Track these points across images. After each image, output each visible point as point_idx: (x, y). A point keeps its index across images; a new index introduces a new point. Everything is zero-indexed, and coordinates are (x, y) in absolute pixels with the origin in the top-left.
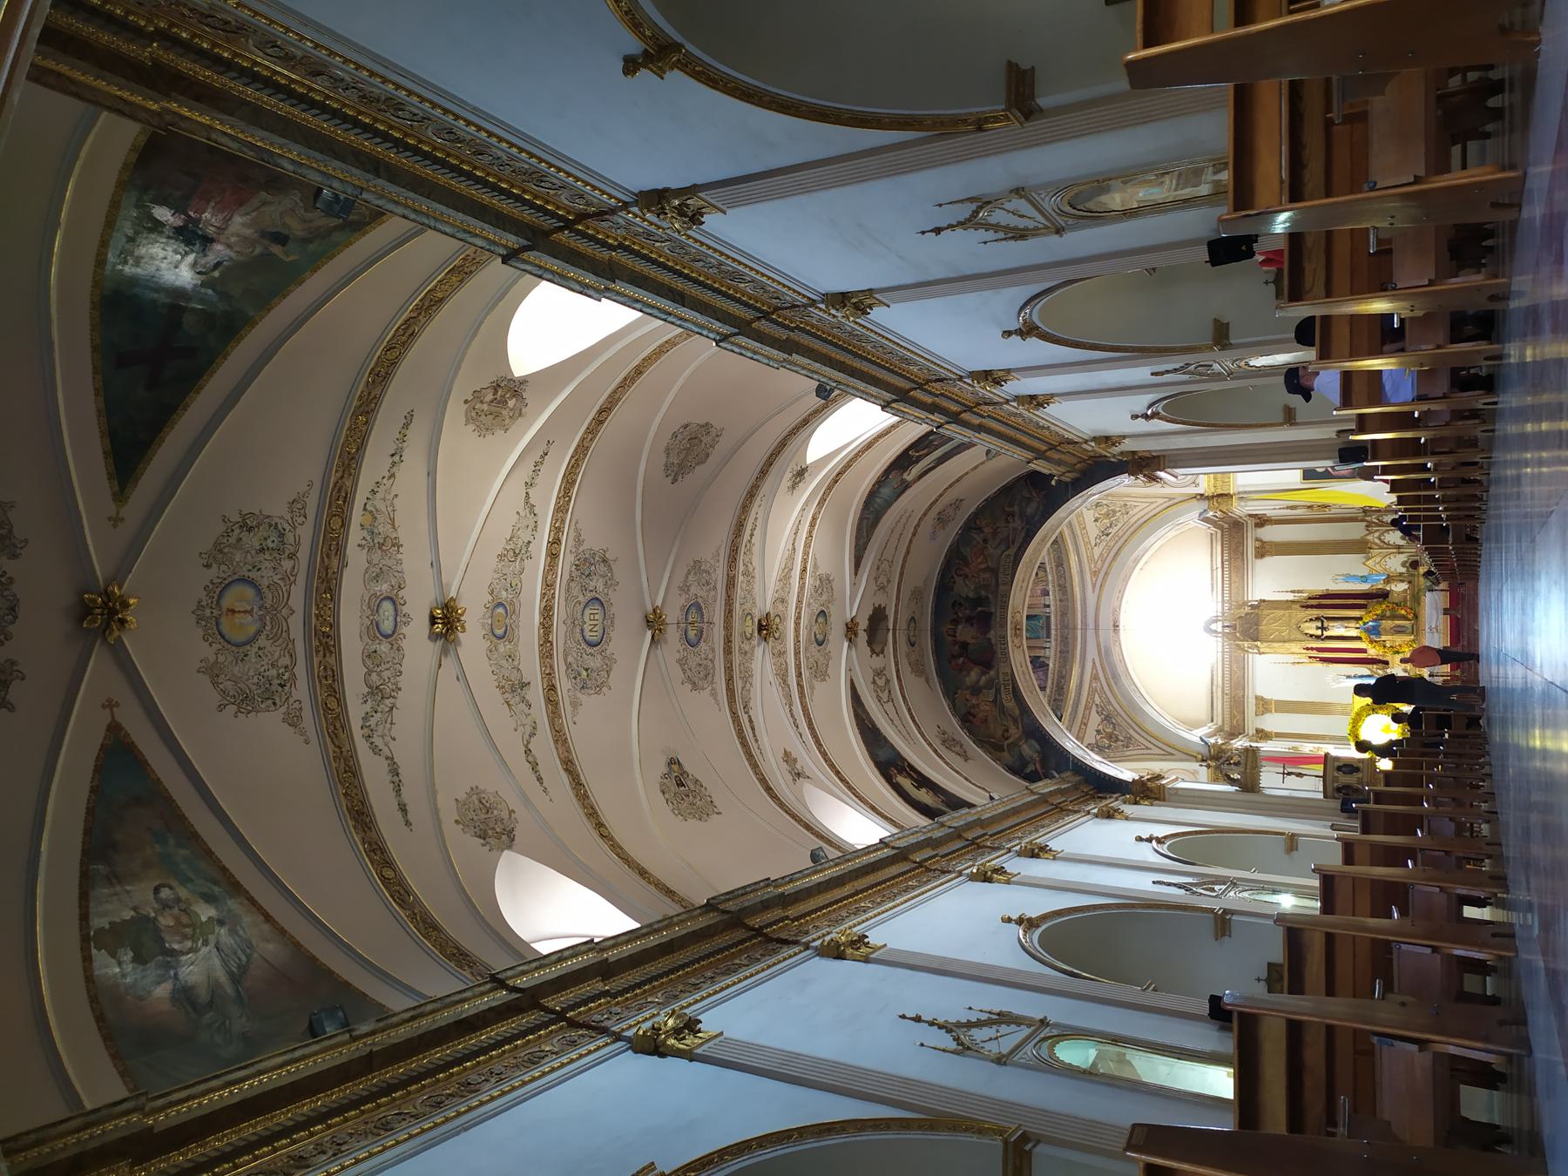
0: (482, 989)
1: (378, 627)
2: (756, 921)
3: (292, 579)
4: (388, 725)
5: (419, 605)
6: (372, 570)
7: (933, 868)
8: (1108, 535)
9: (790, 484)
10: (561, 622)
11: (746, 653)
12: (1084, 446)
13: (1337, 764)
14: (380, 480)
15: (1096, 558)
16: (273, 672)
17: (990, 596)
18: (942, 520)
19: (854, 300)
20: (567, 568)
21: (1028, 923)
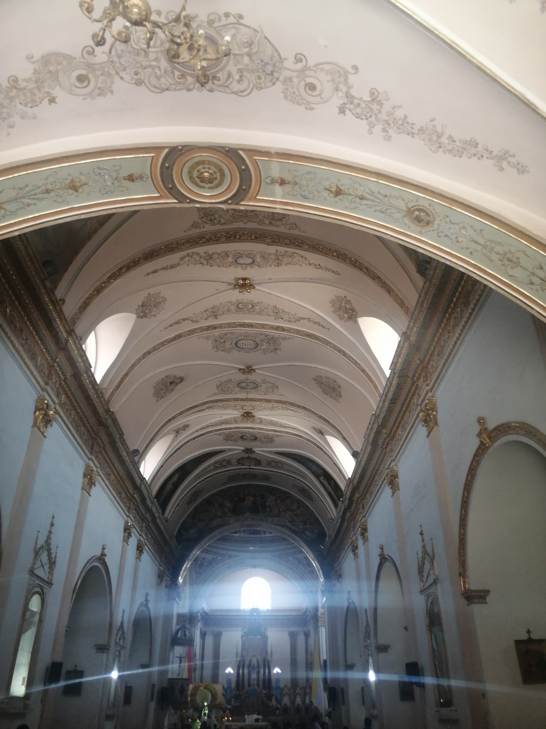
0: (67, 327)
3: (260, 223)
4: (194, 263)
5: (252, 273)
8: (299, 563)
9: (316, 427)
10: (247, 331)
11: (235, 407)
13: (184, 685)
16: (217, 216)
18: (304, 491)
20: (271, 334)
21: (101, 559)
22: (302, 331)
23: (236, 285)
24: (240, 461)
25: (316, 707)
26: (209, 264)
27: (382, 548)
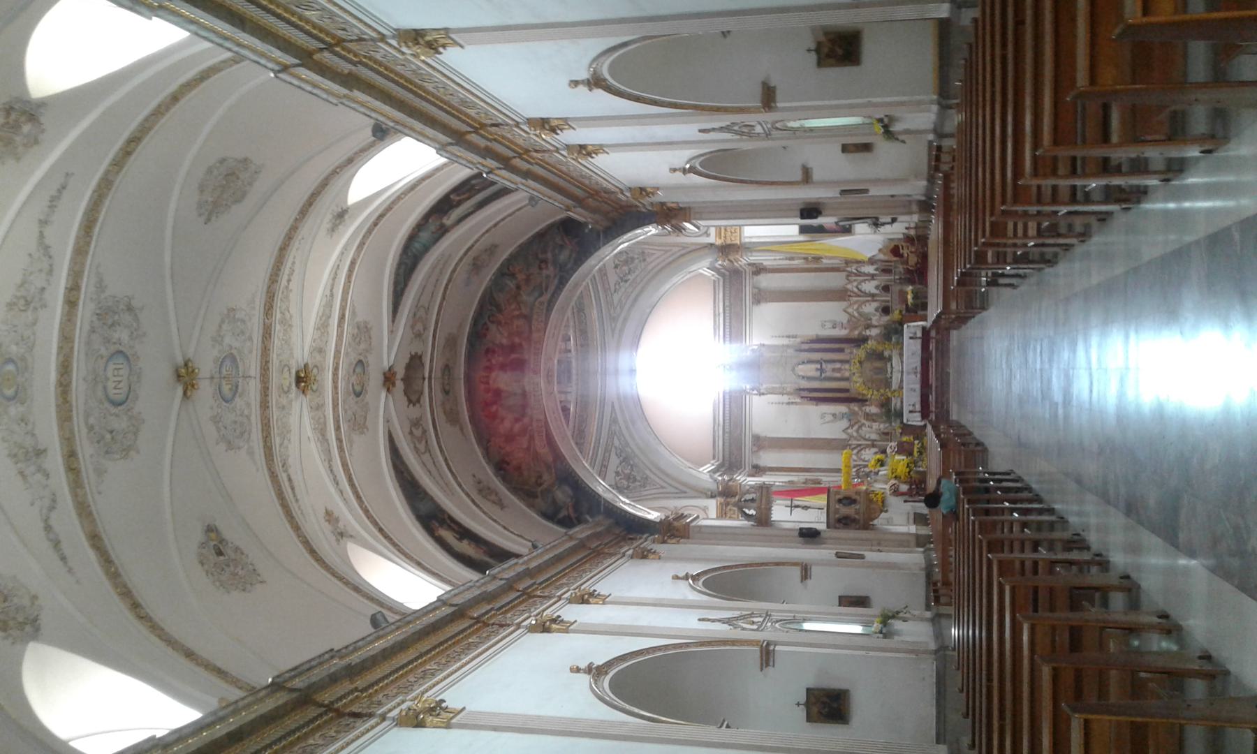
2: (326, 697)
7: (491, 622)
8: (626, 281)
9: (329, 226)
11: (283, 408)
12: (620, 196)
17: (524, 343)
18: (477, 266)
19: (428, 38)
21: (597, 672)
24: (413, 398)
25: (880, 250)
27: (575, 83)
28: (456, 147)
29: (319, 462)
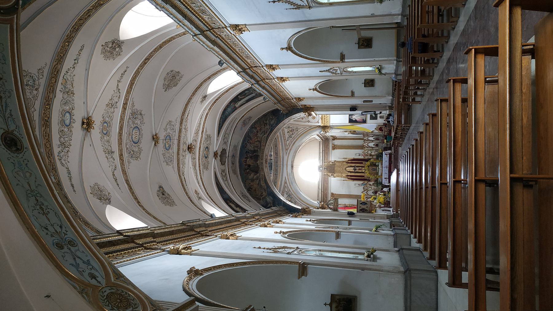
1: (64, 122)
2: (198, 230)
3: (36, 98)
5: (79, 116)
6: (64, 101)
8: (291, 137)
9: (201, 100)
12: (292, 100)
13: (361, 202)
14: (69, 68)
15: (287, 145)
17: (258, 150)
18: (244, 124)
19: (240, 27)
20: (129, 114)
21: (284, 233)
22: (127, 90)
23: (87, 130)
24: (223, 163)
25: (375, 129)
26: (68, 146)
27: (283, 49)
28: (243, 73)
29: (193, 174)
